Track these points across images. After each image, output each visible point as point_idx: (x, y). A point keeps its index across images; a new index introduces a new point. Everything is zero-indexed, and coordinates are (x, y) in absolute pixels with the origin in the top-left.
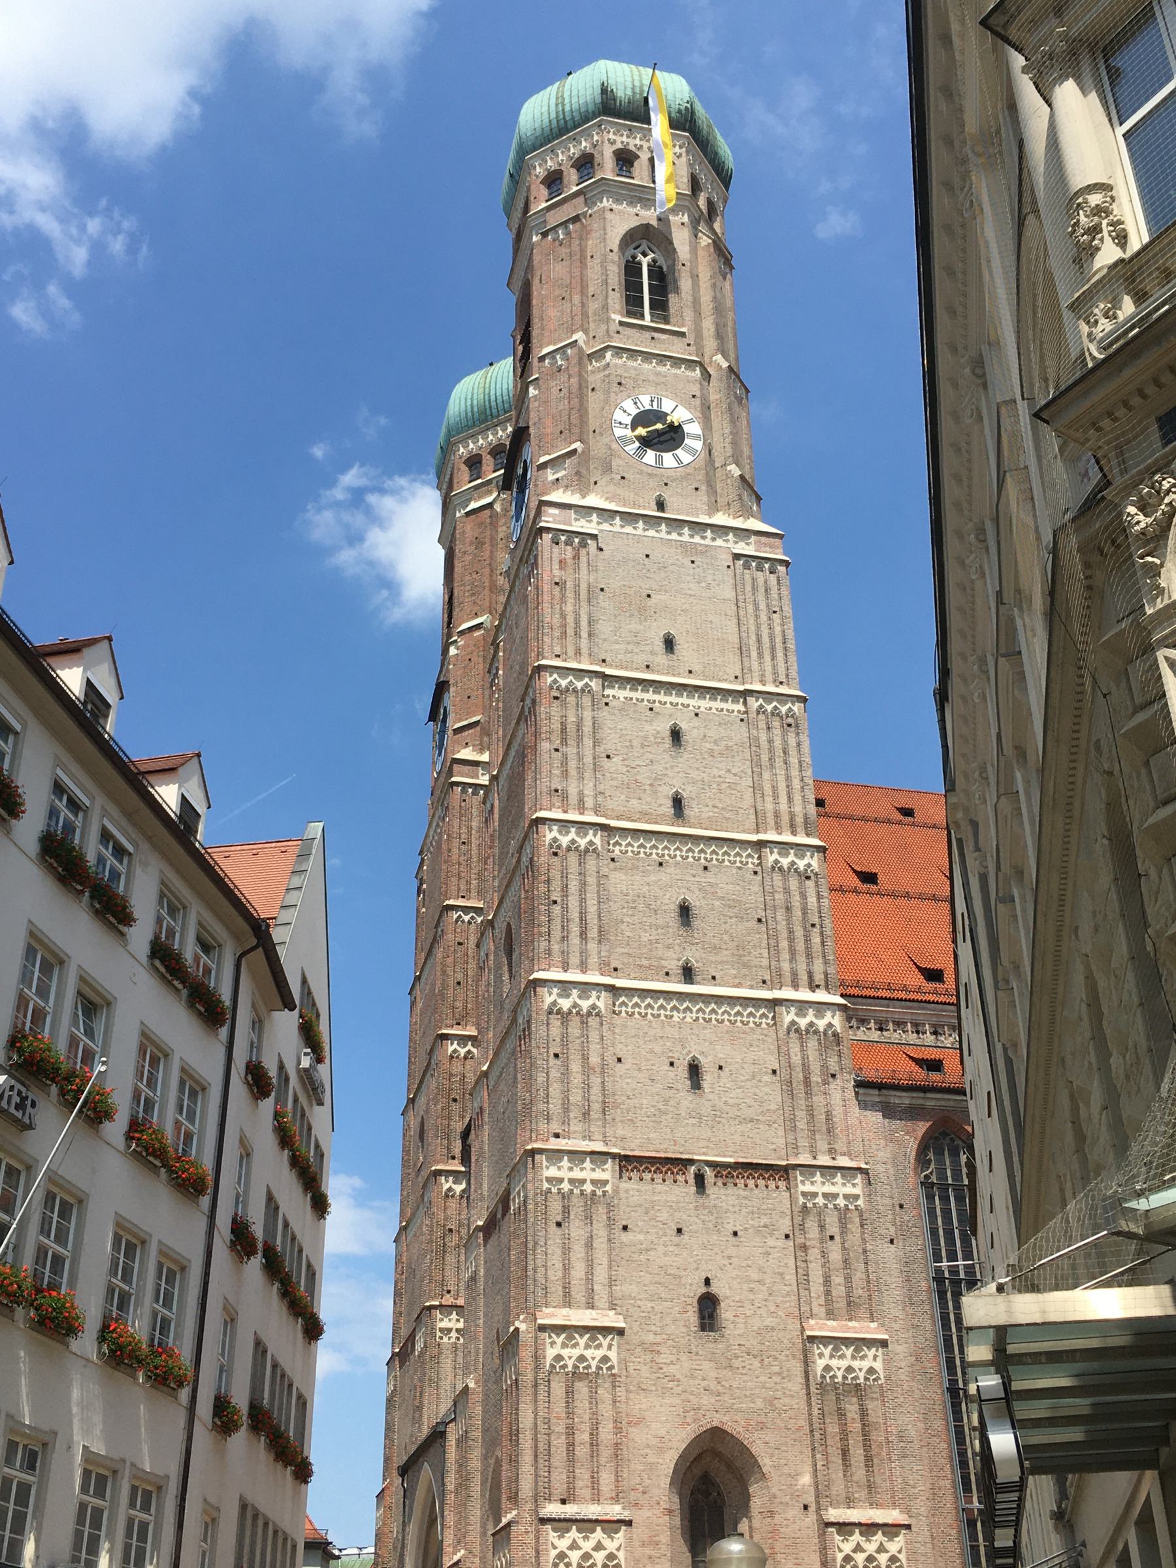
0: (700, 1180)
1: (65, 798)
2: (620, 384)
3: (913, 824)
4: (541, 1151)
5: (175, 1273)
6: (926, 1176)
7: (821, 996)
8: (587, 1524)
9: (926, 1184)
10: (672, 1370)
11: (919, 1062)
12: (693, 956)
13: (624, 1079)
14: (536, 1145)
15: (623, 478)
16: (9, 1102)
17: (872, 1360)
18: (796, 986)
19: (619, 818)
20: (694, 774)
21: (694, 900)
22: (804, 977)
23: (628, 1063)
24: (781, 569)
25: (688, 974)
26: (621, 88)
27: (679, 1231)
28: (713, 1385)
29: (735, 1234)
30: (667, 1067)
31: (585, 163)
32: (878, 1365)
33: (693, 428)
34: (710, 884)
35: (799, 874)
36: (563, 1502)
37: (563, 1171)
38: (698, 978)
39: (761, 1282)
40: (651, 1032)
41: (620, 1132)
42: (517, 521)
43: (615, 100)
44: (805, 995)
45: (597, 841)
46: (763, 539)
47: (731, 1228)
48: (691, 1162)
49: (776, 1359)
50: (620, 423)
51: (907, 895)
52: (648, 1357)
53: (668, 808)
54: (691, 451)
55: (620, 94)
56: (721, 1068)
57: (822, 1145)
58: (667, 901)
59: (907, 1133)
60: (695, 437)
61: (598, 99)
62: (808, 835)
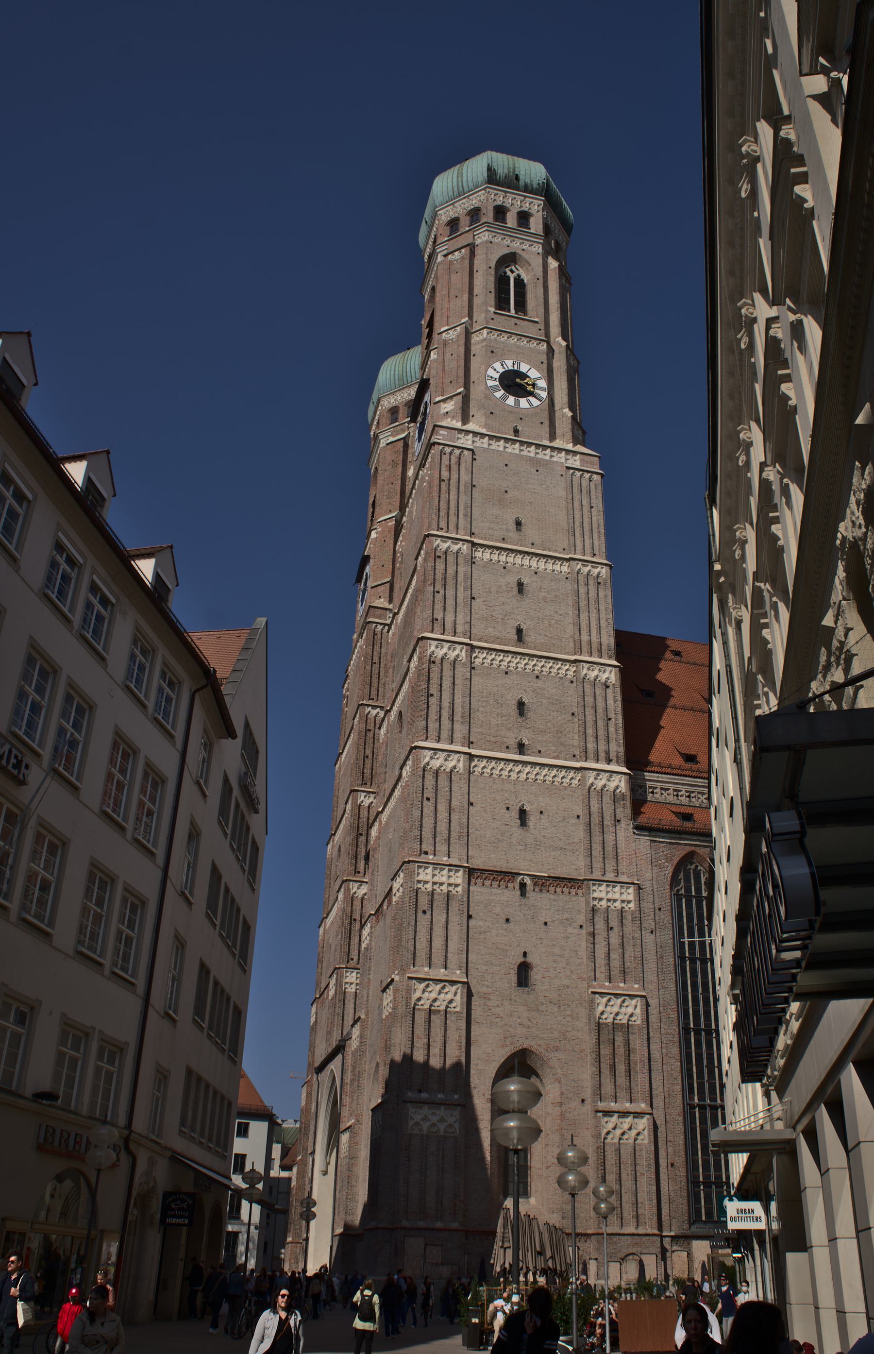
0: (523, 886)
1: (65, 556)
2: (492, 352)
3: (681, 662)
5: (137, 906)
6: (678, 890)
7: (613, 767)
10: (498, 1010)
15: (492, 413)
16: (8, 762)
22: (602, 755)
25: (521, 748)
27: (507, 920)
29: (546, 924)
30: (505, 811)
39: (561, 956)
40: (495, 787)
42: (419, 442)
43: (496, 175)
45: (463, 654)
47: (543, 920)
49: (569, 1006)
50: (491, 377)
56: (541, 812)
58: (509, 698)
59: (667, 861)
61: (486, 174)
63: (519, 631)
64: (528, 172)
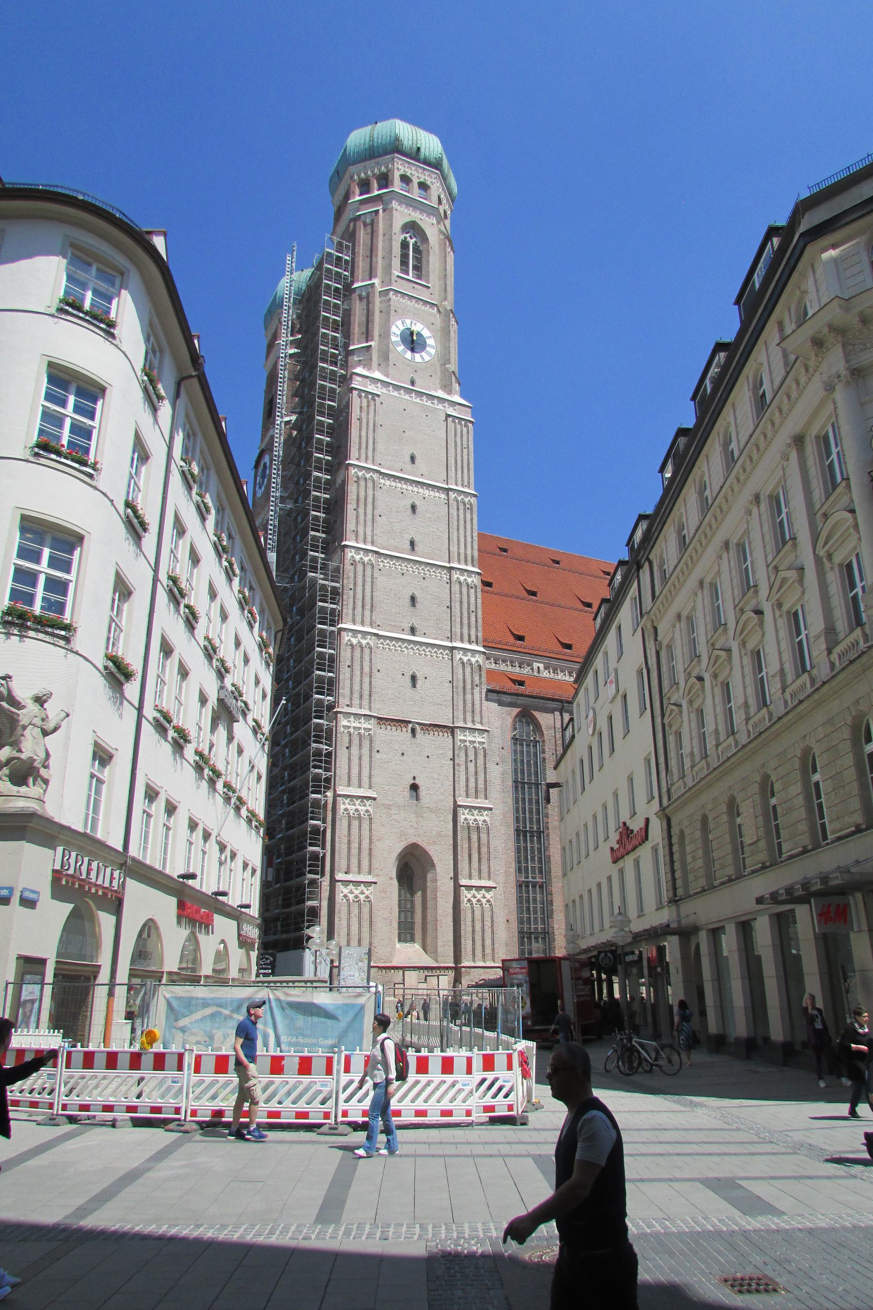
0: (413, 731)
4: (340, 712)
7: (474, 647)
8: (357, 883)
9: (514, 739)
10: (396, 817)
11: (514, 681)
13: (379, 680)
14: (339, 710)
17: (485, 816)
18: (462, 641)
19: (383, 548)
21: (418, 595)
22: (466, 637)
24: (470, 425)
25: (413, 631)
28: (414, 824)
31: (385, 180)
32: (487, 819)
33: (430, 342)
35: (468, 586)
37: (354, 723)
38: (417, 633)
41: (378, 706)
44: (466, 646)
46: (462, 408)
48: (410, 722)
51: (506, 595)
53: (407, 546)
54: (429, 354)
55: (405, 143)
57: (469, 717)
60: (432, 347)
62: (473, 566)
63: (412, 543)
64: (427, 145)
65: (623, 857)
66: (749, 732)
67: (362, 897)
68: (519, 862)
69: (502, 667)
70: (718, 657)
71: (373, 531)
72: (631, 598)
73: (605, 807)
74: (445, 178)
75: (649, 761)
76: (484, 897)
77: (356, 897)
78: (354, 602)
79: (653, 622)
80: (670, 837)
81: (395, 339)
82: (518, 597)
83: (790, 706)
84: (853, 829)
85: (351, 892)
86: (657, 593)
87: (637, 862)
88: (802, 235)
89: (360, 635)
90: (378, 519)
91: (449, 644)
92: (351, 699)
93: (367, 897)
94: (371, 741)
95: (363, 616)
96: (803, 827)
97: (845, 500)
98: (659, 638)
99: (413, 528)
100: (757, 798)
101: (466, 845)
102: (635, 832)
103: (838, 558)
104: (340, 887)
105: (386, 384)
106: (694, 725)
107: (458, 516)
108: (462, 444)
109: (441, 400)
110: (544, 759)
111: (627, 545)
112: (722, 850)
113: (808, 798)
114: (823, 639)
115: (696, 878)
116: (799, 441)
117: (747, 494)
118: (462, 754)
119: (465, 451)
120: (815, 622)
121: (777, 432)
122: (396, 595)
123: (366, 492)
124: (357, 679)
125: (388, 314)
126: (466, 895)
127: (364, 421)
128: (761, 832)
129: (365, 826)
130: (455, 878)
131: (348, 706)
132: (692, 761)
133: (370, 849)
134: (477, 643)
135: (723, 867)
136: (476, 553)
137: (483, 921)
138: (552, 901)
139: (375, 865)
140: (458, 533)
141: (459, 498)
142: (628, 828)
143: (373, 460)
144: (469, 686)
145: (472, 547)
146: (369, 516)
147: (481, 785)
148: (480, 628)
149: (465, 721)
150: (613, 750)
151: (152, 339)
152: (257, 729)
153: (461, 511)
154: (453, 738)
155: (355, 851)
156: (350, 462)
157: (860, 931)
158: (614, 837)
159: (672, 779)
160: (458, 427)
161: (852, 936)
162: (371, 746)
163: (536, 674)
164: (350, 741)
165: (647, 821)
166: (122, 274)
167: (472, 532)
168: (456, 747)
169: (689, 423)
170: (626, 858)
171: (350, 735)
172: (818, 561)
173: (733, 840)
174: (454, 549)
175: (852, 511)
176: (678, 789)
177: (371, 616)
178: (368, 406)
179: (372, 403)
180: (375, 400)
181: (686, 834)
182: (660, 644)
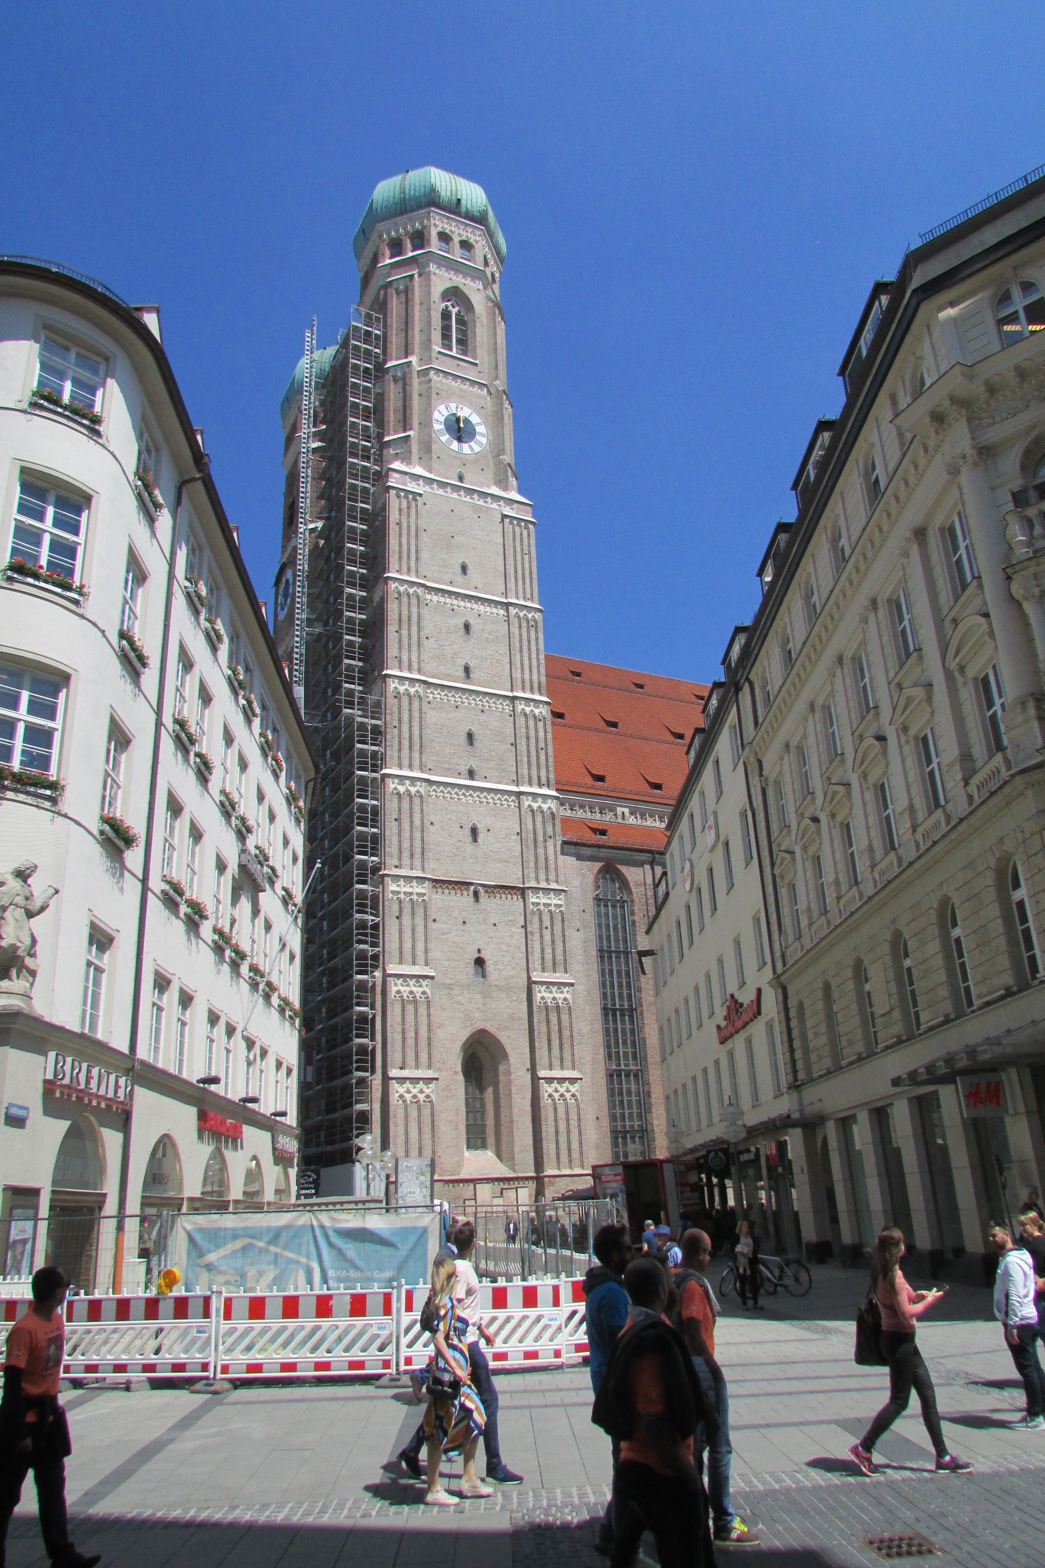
0: (476, 894)
4: (388, 875)
8: (415, 1080)
9: (597, 899)
10: (460, 998)
12: (474, 764)
13: (433, 835)
14: (385, 872)
17: (566, 994)
18: (530, 784)
19: (433, 677)
20: (477, 653)
21: (475, 730)
22: (535, 779)
23: (437, 826)
24: (531, 526)
25: (471, 774)
26: (444, 189)
27: (464, 922)
30: (459, 829)
31: (420, 239)
32: (568, 996)
33: (481, 429)
34: (485, 721)
36: (401, 1068)
37: (404, 888)
38: (476, 777)
39: (507, 951)
41: (432, 866)
46: (521, 507)
47: (492, 921)
48: (471, 884)
51: (580, 728)
52: (447, 991)
53: (461, 673)
54: (480, 444)
55: (443, 194)
60: (482, 435)
62: (541, 694)
63: (467, 670)
65: (731, 1036)
66: (875, 881)
67: (421, 1097)
68: (609, 1047)
69: (580, 814)
70: (835, 793)
71: (419, 656)
72: (730, 727)
73: (708, 977)
74: (490, 234)
75: (758, 920)
76: (568, 1091)
77: (415, 1096)
78: (400, 743)
79: (756, 753)
80: (787, 1010)
81: (438, 427)
82: (596, 730)
83: (923, 848)
84: (1002, 992)
85: (408, 1091)
86: (760, 720)
87: (749, 1041)
88: (914, 291)
89: (408, 782)
90: (425, 642)
91: (515, 789)
92: (400, 859)
93: (428, 1096)
94: (425, 908)
95: (410, 759)
96: (944, 992)
97: (977, 603)
98: (764, 773)
99: (468, 652)
100: (888, 960)
101: (544, 1029)
102: (745, 1006)
103: (971, 672)
104: (394, 1086)
105: (429, 481)
106: (809, 875)
107: (521, 635)
108: (522, 550)
109: (496, 498)
110: (634, 922)
111: (723, 663)
112: (849, 1024)
113: (948, 959)
114: (958, 767)
115: (820, 1058)
116: (920, 534)
117: (861, 599)
118: (536, 920)
119: (526, 557)
120: (947, 749)
121: (894, 525)
122: (449, 732)
123: (409, 611)
124: (406, 834)
125: (429, 398)
126: (546, 1089)
127: (405, 525)
128: (895, 1000)
129: (423, 1011)
130: (533, 1069)
131: (396, 867)
132: (810, 918)
133: (429, 1039)
134: (548, 786)
135: (851, 1043)
136: (543, 679)
137: (568, 1120)
138: (649, 1092)
139: (436, 1057)
140: (522, 656)
141: (521, 614)
142: (736, 1001)
143: (417, 572)
144: (540, 838)
145: (539, 672)
146: (415, 639)
147: (560, 957)
148: (551, 769)
149: (537, 880)
150: (716, 909)
151: (146, 436)
152: (287, 899)
153: (524, 630)
154: (524, 901)
155: (410, 1042)
156: (390, 575)
157: (1016, 1114)
158: (721, 1012)
159: (786, 941)
160: (517, 529)
161: (1007, 1120)
162: (426, 915)
163: (620, 820)
164: (401, 910)
165: (759, 991)
166: (107, 359)
167: (538, 654)
168: (528, 912)
169: (791, 515)
170: (736, 1037)
171: (400, 902)
172: (949, 676)
173: (862, 1010)
174: (517, 675)
175: (986, 615)
176: (794, 952)
177: (421, 759)
178: (408, 508)
179: (413, 504)
180: (416, 500)
181: (806, 1006)
182: (766, 780)
